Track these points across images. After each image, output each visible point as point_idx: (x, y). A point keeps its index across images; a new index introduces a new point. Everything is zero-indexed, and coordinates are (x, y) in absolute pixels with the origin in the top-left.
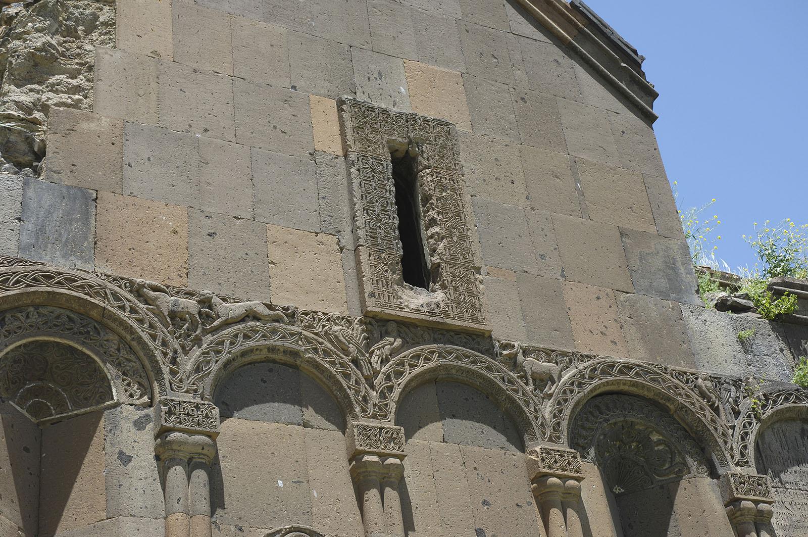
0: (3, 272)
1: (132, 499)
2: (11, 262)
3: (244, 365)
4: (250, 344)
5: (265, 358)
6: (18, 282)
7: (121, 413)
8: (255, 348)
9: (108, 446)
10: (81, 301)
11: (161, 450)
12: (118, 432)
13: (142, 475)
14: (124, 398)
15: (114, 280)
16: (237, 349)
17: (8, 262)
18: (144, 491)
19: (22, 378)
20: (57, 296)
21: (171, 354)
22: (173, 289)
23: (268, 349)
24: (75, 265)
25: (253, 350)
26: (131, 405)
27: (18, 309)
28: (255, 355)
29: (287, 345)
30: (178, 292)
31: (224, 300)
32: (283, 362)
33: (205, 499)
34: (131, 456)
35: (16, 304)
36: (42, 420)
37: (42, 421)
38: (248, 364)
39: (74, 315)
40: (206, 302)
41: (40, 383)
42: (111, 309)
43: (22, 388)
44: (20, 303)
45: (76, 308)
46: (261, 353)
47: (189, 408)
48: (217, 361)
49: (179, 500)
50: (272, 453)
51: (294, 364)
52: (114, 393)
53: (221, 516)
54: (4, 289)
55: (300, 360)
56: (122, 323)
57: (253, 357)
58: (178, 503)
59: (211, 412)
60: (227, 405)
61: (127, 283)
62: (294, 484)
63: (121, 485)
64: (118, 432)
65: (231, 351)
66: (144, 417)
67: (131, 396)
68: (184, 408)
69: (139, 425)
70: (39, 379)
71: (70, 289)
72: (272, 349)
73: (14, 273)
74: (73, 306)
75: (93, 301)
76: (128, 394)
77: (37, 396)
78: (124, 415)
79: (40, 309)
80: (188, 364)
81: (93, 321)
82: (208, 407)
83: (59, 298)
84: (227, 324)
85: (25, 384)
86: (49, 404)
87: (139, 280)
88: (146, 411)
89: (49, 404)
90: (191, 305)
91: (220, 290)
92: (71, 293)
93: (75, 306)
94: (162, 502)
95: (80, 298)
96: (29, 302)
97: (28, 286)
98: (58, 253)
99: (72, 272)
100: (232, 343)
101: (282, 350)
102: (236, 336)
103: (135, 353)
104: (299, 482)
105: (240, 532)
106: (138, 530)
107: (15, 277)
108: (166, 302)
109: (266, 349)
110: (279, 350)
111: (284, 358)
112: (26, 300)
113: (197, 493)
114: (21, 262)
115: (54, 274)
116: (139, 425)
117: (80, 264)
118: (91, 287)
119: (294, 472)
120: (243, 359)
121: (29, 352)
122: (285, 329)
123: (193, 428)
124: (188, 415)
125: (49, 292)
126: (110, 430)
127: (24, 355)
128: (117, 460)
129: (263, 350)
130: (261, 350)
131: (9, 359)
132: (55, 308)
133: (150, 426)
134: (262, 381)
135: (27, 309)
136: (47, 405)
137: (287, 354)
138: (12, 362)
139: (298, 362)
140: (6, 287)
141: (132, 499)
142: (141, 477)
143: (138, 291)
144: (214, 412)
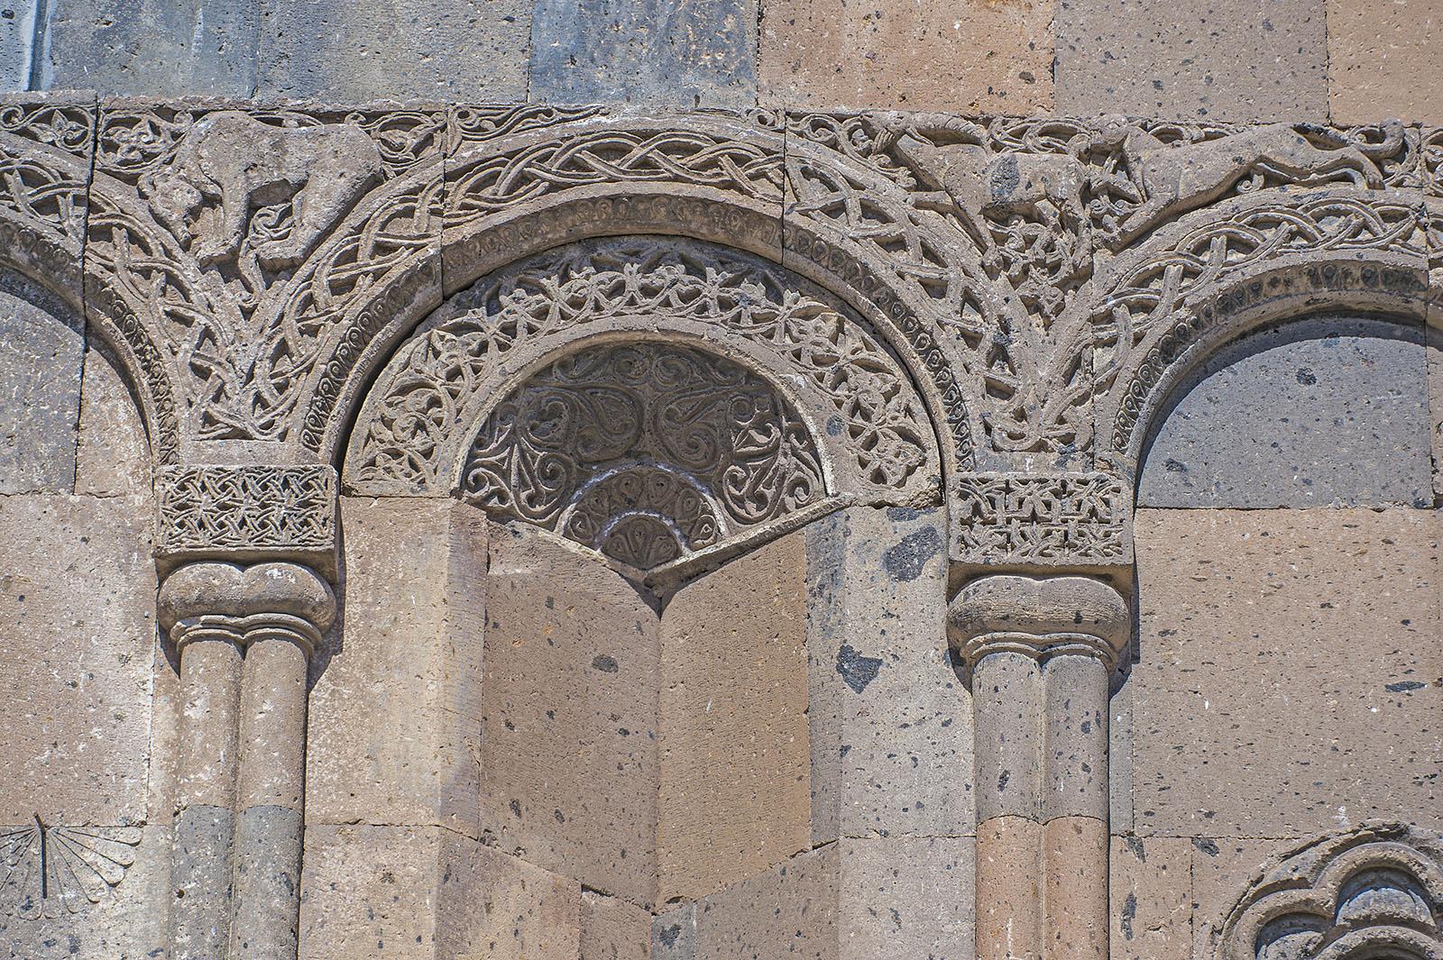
0: (477, 159)
1: (880, 787)
2: (505, 121)
3: (1243, 336)
4: (1256, 266)
5: (1308, 303)
6: (523, 179)
7: (847, 533)
8: (1266, 280)
9: (815, 632)
10: (711, 209)
11: (958, 634)
12: (838, 593)
13: (908, 712)
14: (858, 487)
15: (816, 125)
16: (1205, 290)
17: (498, 124)
18: (915, 759)
19: (571, 459)
20: (641, 207)
21: (990, 334)
22: (1004, 123)
23: (1313, 275)
24: (697, 98)
25: (1261, 286)
26: (878, 506)
27: (537, 259)
28: (1271, 300)
29: (1371, 255)
30: (1019, 134)
31: (1169, 136)
32: (1371, 308)
33: (1086, 768)
34: (876, 660)
35: (526, 247)
36: (657, 570)
37: (657, 575)
38: (1255, 330)
39: (701, 251)
40: (1111, 152)
41: (632, 466)
42: (802, 222)
43: (578, 487)
44: (537, 241)
45: (704, 230)
46: (1292, 290)
47: (1036, 498)
48: (1138, 339)
49: (1004, 778)
50: (1323, 606)
51: (1404, 311)
52: (829, 477)
53: (1148, 813)
54: (481, 209)
55: (1422, 295)
56: (838, 258)
57: (1264, 308)
58: (1001, 788)
59: (1107, 502)
60: (1182, 469)
61: (855, 129)
62: (1392, 695)
63: (845, 749)
64: (838, 593)
65: (1182, 300)
66: (916, 537)
67: (879, 477)
68: (1021, 502)
69: (900, 564)
70: (628, 454)
71: (677, 179)
72: (1323, 274)
73: (510, 155)
74: (693, 226)
75: (745, 205)
76: (868, 472)
77: (632, 504)
78: (855, 538)
79: (600, 250)
80: (1040, 356)
81: (760, 262)
82: (1098, 489)
83: (646, 210)
84: (1174, 211)
85: (589, 476)
86: (668, 523)
87: (890, 116)
88: (923, 520)
89: (668, 523)
90: (1057, 172)
91: (1160, 105)
92: (680, 191)
93: (698, 225)
94: (968, 787)
95: (706, 203)
96: (564, 234)
97: (555, 187)
98: (645, 68)
99: (684, 123)
100: (1189, 273)
101: (1357, 273)
102: (1204, 246)
103: (889, 345)
104: (1410, 686)
105: (1205, 855)
106: (895, 873)
107: (514, 165)
108: (973, 174)
109: (1305, 278)
110: (1347, 274)
111: (1366, 297)
112: (553, 230)
113: (1060, 754)
114: (534, 115)
115: (630, 139)
116: (900, 564)
117: (710, 91)
118: (739, 160)
119: (1394, 656)
120: (1231, 317)
121: (581, 382)
122: (1367, 203)
123: (1047, 561)
124: (1034, 517)
125: (614, 199)
126: (821, 587)
127: (565, 393)
128: (837, 674)
129: (1297, 282)
130: (1288, 283)
131: (522, 410)
132: (643, 240)
133: (935, 564)
134: (1299, 379)
135: (562, 255)
136: (664, 526)
137: (1375, 284)
138: (531, 418)
139: (1417, 306)
140: (486, 200)
141: (880, 787)
142: (906, 720)
143: (890, 149)
144: (1114, 501)
